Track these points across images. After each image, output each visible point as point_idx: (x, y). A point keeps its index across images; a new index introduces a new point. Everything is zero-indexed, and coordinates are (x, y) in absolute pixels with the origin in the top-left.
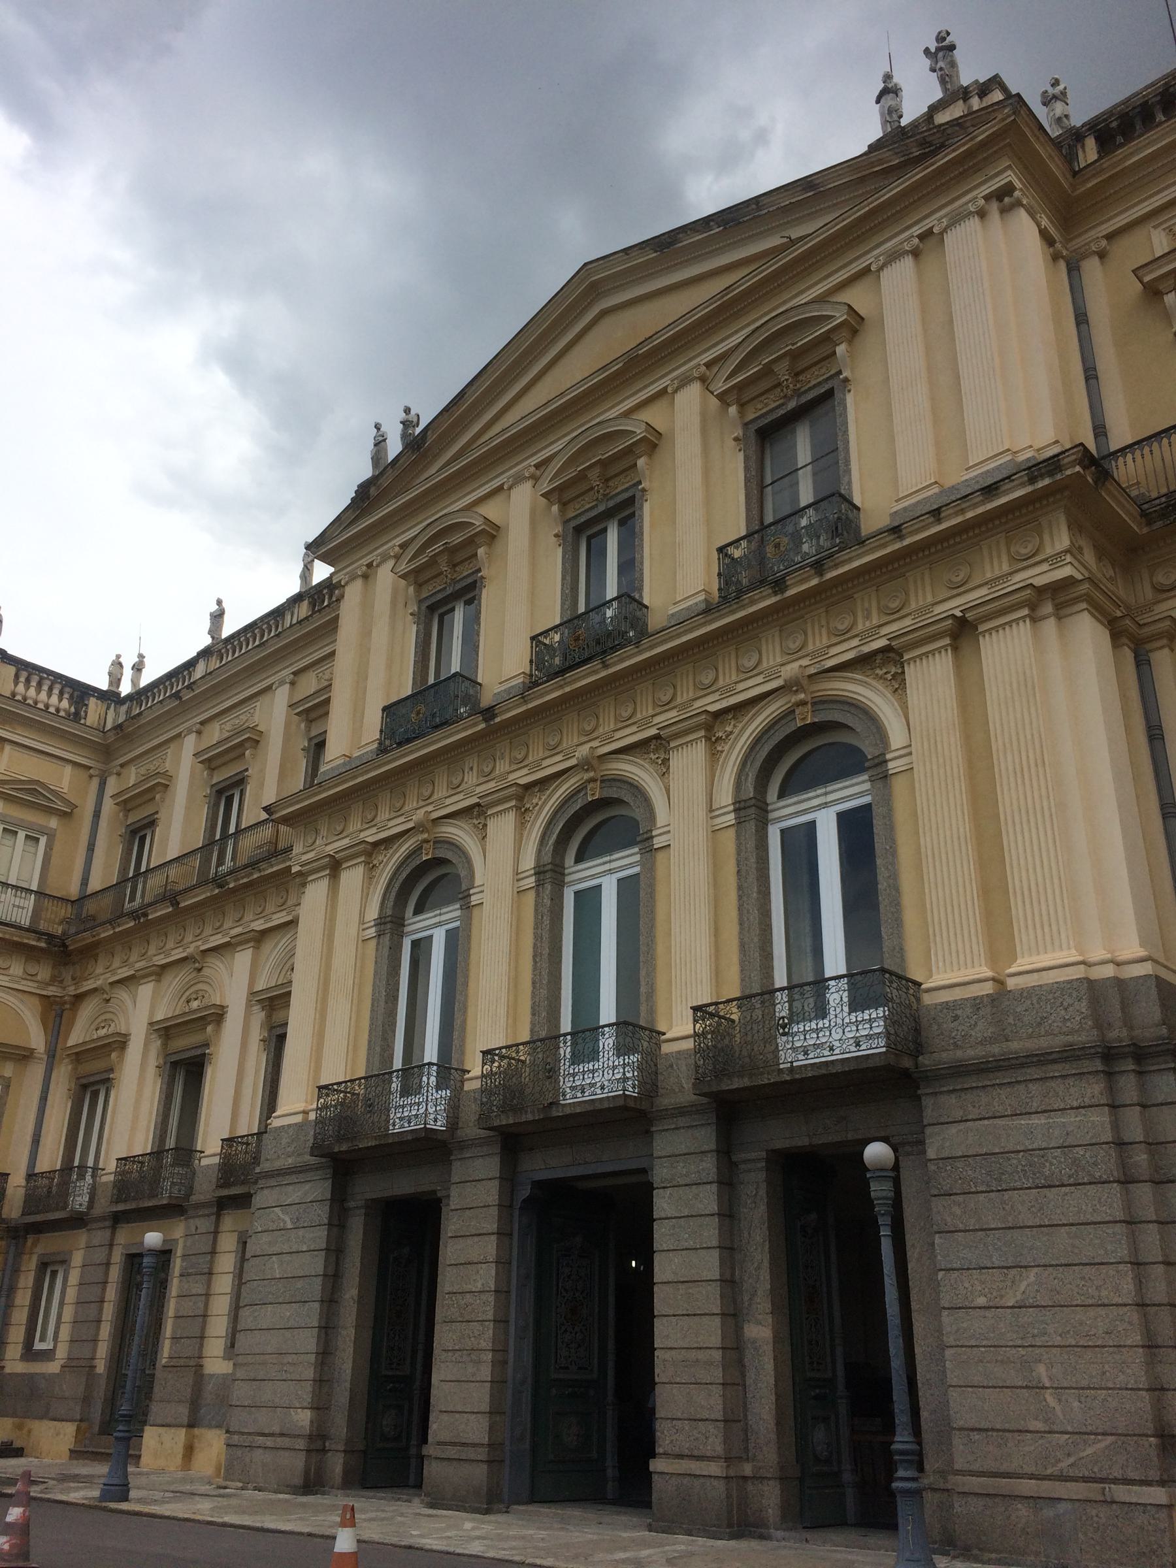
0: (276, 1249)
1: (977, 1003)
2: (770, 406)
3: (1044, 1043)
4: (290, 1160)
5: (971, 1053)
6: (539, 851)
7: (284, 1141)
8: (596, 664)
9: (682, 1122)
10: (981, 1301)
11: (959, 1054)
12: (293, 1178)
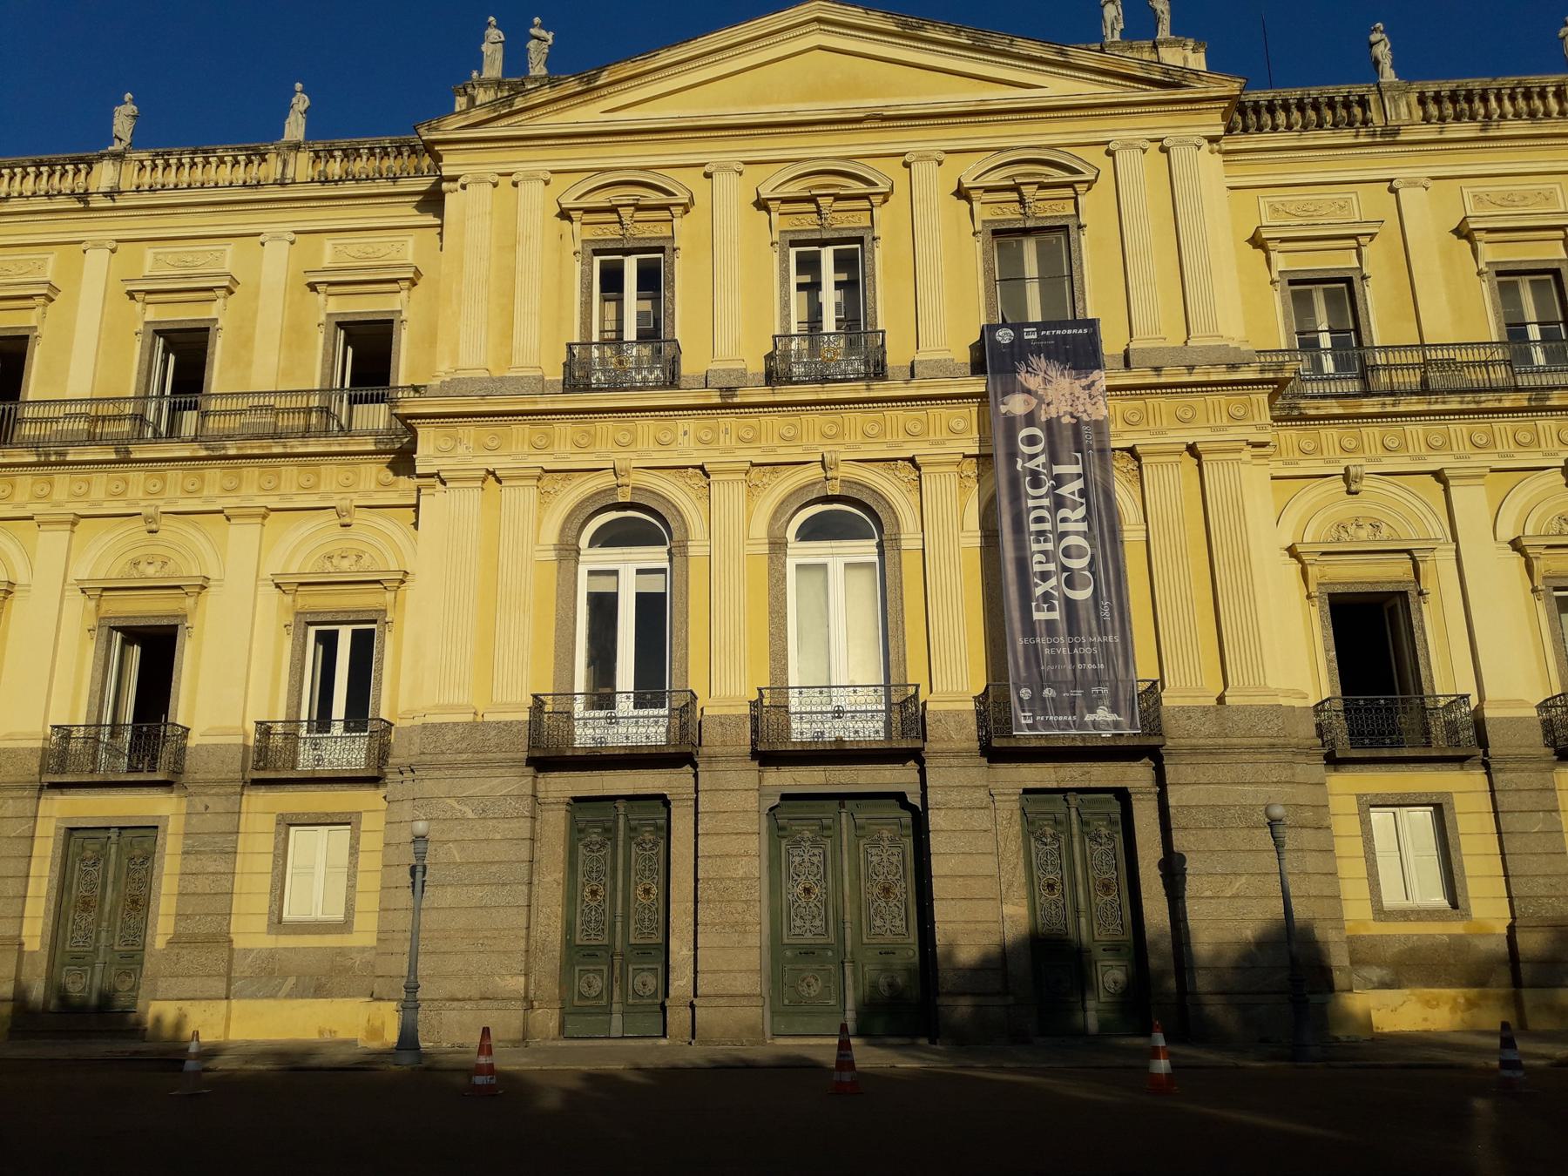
0: (453, 836)
1: (1205, 710)
2: (1010, 214)
3: (1255, 741)
4: (464, 756)
5: (1202, 741)
6: (771, 526)
7: (449, 738)
8: (861, 385)
9: (954, 762)
10: (1208, 893)
11: (1194, 741)
12: (473, 772)
